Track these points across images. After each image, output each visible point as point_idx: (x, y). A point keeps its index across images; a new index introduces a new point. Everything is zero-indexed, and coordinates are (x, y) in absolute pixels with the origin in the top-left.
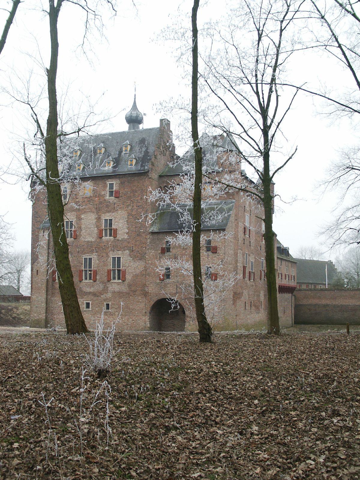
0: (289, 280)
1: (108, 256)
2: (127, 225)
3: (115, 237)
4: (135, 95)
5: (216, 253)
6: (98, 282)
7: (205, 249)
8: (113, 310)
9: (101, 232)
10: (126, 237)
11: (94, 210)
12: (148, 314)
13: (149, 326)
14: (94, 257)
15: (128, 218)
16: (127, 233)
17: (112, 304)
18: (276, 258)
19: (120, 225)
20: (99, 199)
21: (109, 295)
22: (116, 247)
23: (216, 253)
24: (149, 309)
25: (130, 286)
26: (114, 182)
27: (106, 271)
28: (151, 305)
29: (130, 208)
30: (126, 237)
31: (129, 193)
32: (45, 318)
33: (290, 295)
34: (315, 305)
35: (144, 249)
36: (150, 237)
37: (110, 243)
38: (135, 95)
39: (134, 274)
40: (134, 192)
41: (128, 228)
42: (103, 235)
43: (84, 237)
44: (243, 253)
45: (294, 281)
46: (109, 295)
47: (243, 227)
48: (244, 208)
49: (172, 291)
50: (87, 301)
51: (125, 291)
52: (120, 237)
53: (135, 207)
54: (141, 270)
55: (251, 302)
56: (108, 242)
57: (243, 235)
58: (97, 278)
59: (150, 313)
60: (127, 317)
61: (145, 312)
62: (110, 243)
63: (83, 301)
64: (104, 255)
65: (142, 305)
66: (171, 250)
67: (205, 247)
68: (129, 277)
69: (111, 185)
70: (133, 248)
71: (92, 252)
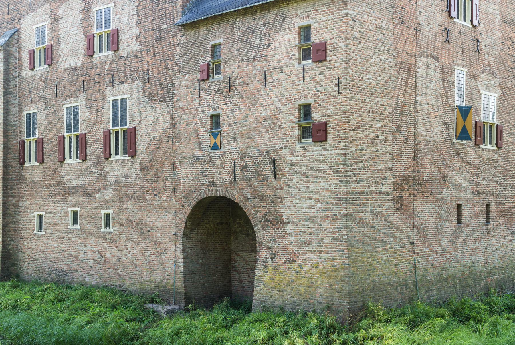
2: (137, 18)
3: (117, 50)
5: (325, 60)
6: (89, 163)
7: (297, 55)
8: (116, 228)
9: (90, 40)
10: (136, 47)
12: (180, 239)
13: (182, 269)
21: (109, 193)
23: (325, 60)
24: (182, 226)
25: (144, 168)
27: (102, 134)
28: (186, 216)
30: (136, 47)
35: (170, 72)
36: (180, 40)
37: (107, 67)
39: (152, 136)
43: (64, 59)
44: (442, 68)
46: (109, 193)
49: (225, 177)
51: (136, 182)
52: (123, 51)
54: (165, 125)
55: (488, 206)
58: (88, 152)
59: (184, 235)
61: (175, 234)
65: (169, 217)
67: (297, 48)
68: (142, 147)
70: (148, 74)
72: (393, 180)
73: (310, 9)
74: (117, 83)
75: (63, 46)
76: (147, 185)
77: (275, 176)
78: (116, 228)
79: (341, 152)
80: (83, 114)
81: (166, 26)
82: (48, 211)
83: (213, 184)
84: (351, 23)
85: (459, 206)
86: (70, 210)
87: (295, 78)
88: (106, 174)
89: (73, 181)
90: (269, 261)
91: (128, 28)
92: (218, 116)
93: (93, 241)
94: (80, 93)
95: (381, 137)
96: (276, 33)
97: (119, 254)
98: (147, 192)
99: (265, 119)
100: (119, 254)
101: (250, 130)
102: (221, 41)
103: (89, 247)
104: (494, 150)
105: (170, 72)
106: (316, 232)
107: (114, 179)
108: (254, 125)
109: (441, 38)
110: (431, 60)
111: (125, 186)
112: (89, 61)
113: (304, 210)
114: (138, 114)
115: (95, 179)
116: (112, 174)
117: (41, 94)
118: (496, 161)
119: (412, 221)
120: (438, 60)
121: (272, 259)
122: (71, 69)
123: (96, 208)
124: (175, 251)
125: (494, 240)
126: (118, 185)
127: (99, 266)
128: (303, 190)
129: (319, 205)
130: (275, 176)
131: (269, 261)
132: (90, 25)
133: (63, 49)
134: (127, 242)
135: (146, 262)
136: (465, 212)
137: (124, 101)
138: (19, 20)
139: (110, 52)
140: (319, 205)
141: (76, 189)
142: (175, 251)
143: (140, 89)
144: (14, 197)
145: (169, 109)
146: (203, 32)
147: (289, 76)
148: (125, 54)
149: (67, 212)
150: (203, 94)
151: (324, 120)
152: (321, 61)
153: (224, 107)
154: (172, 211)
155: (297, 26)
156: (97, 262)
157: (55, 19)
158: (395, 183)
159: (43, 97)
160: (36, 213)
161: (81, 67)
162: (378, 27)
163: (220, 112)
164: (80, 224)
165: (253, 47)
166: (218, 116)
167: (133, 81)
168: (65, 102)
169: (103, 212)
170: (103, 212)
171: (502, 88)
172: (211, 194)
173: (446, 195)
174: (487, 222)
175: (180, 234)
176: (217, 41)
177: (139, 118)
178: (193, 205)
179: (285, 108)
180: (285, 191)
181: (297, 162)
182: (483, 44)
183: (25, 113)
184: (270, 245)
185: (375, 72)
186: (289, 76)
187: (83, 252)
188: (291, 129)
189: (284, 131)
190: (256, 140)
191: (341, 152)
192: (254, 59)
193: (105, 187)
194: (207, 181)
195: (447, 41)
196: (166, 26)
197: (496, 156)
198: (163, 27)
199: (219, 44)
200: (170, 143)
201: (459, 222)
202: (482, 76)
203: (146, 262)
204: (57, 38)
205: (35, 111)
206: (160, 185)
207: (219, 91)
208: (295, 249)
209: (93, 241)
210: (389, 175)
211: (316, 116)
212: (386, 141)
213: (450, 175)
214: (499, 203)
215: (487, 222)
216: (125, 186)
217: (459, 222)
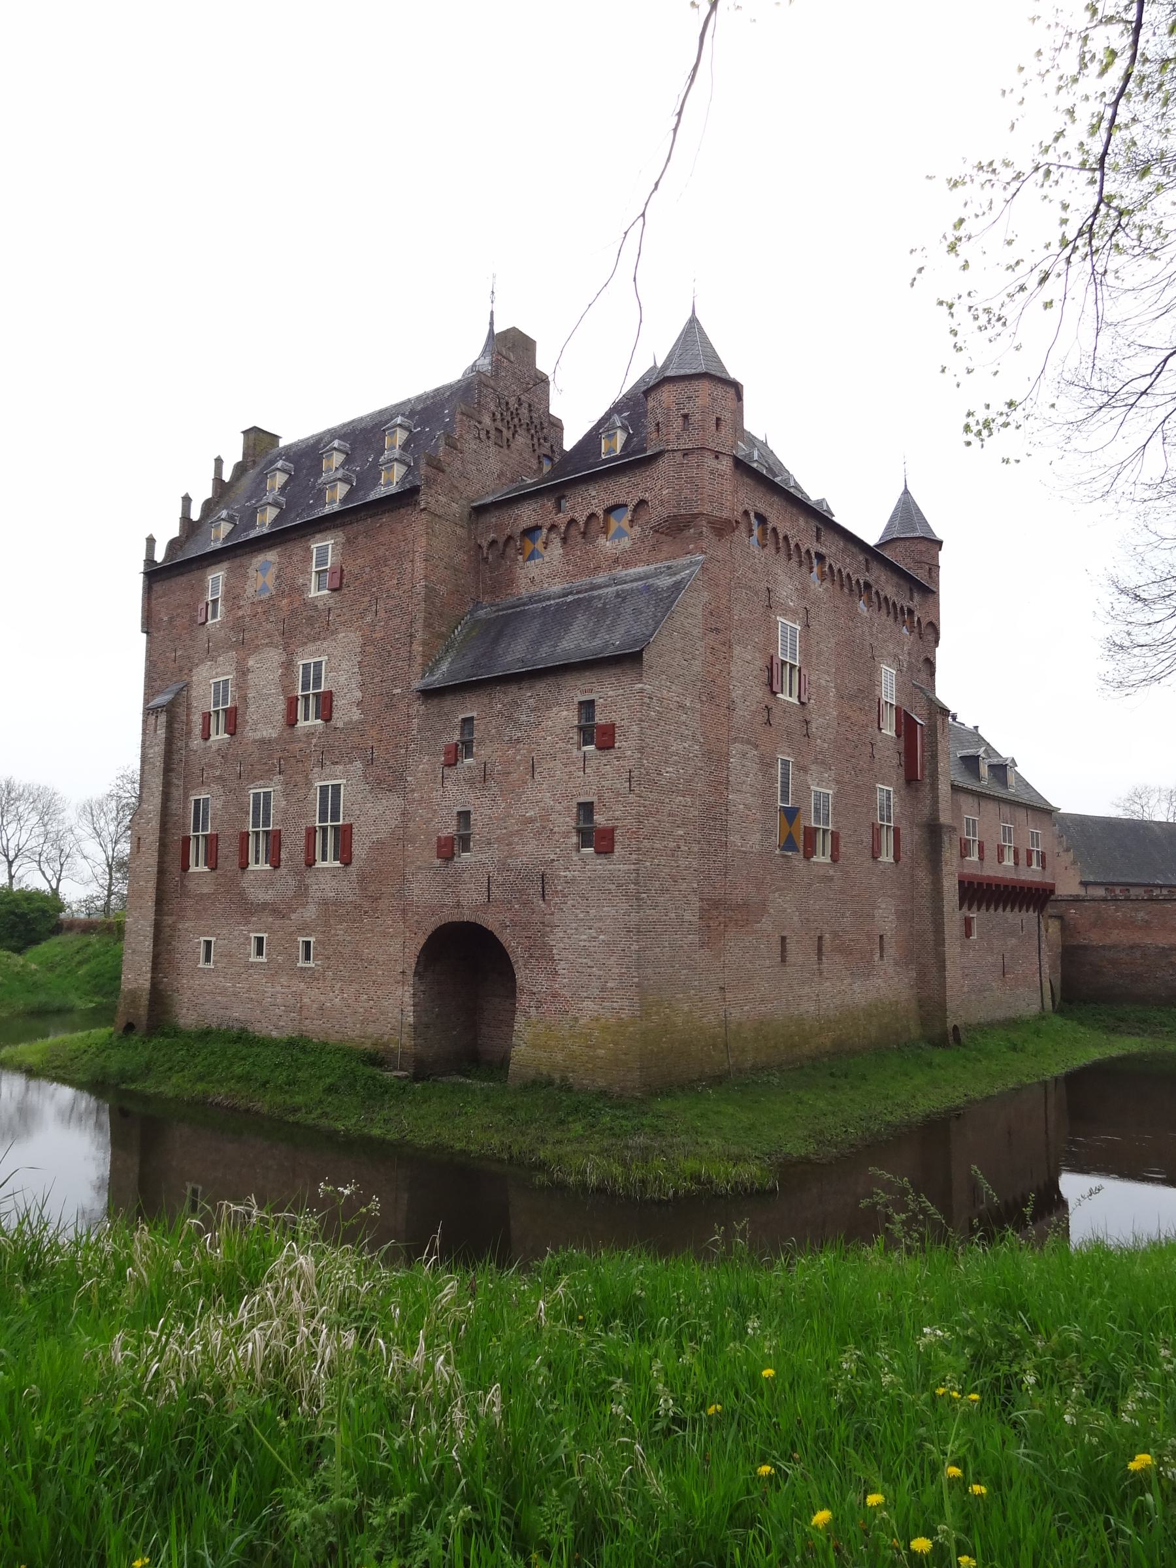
0: (1016, 864)
1: (309, 783)
2: (360, 677)
3: (328, 719)
4: (492, 313)
5: (613, 747)
6: (283, 870)
7: (576, 737)
8: (319, 962)
9: (292, 703)
10: (356, 715)
11: (278, 639)
12: (411, 979)
13: (411, 1020)
14: (274, 787)
15: (363, 652)
16: (359, 704)
17: (317, 942)
18: (944, 788)
19: (342, 679)
20: (291, 603)
21: (310, 912)
22: (327, 755)
23: (613, 747)
24: (413, 961)
25: (363, 879)
26: (330, 542)
27: (304, 832)
28: (420, 948)
29: (368, 619)
30: (356, 715)
31: (367, 569)
32: (147, 985)
33: (1032, 915)
34: (1132, 947)
35: (403, 751)
36: (418, 711)
37: (314, 741)
38: (492, 313)
39: (375, 837)
40: (379, 563)
41: (362, 685)
42: (299, 718)
43: (253, 727)
44: (762, 757)
45: (1044, 868)
46: (310, 912)
47: (760, 663)
48: (764, 596)
49: (475, 896)
50: (257, 931)
51: (350, 899)
52: (339, 719)
53: (382, 614)
54: (394, 823)
55: (820, 938)
56: (310, 735)
57: (760, 693)
58: (283, 856)
59: (416, 973)
60: (355, 986)
61: (403, 972)
62: (314, 741)
63: (249, 932)
64: (299, 778)
65: (395, 947)
66: (475, 749)
67: (576, 730)
68: (359, 849)
69: (323, 551)
70: (372, 753)
71: (267, 774)
72: (698, 904)
73: (594, 680)
74: (328, 763)
75: (252, 709)
76: (366, 905)
77: (543, 896)
78: (319, 962)
79: (633, 867)
80: (277, 803)
81: (399, 691)
82: (220, 937)
83: (458, 905)
84: (647, 700)
85: (783, 939)
86: (253, 935)
87: (573, 768)
88: (307, 887)
89: (260, 895)
90: (533, 1011)
91: (346, 690)
92: (468, 813)
93: (284, 980)
94: (274, 775)
95: (683, 848)
96: (549, 708)
97: (322, 998)
98: (366, 912)
99: (532, 820)
100: (322, 998)
101: (512, 834)
102: (474, 714)
103: (279, 988)
104: (827, 864)
105: (403, 751)
106: (598, 973)
107: (319, 894)
108: (516, 828)
109: (761, 719)
110: (747, 748)
111: (334, 904)
112: (289, 732)
113: (582, 943)
114: (356, 807)
115: (290, 893)
116: (317, 887)
117: (218, 773)
118: (831, 879)
119: (722, 959)
120: (756, 747)
121: (537, 1008)
122: (263, 741)
123: (291, 933)
124: (403, 995)
125: (828, 984)
126: (324, 903)
127: (292, 1014)
128: (581, 916)
129: (602, 937)
130: (543, 896)
131: (533, 1011)
132: (293, 683)
133: (252, 714)
134: (334, 982)
135: (361, 1010)
136: (791, 946)
137: (336, 788)
138: (191, 670)
139: (319, 721)
140: (602, 937)
141: (264, 906)
142: (403, 995)
143: (360, 773)
144: (172, 915)
145: (400, 801)
146: (448, 703)
147: (565, 765)
148: (340, 725)
149: (248, 938)
150: (446, 784)
151: (610, 824)
152: (608, 748)
153: (478, 802)
154: (400, 940)
155: (576, 700)
156: (288, 1009)
157: (243, 672)
158: (701, 909)
159: (220, 778)
160: (202, 939)
161: (277, 740)
162: (681, 706)
163: (471, 809)
164: (268, 955)
165: (517, 725)
166: (468, 813)
167: (351, 762)
168: (252, 786)
169: (301, 939)
170: (301, 939)
171: (838, 782)
172: (455, 919)
173: (766, 924)
174: (820, 959)
175: (410, 972)
176: (469, 715)
177: (358, 812)
178: (429, 933)
179: (558, 807)
180: (557, 916)
181: (574, 879)
182: (814, 725)
183: (193, 798)
184: (535, 990)
185: (676, 763)
186: (565, 765)
187: (269, 995)
188: (566, 835)
189: (556, 837)
190: (519, 847)
191: (633, 867)
192: (518, 741)
193: (304, 905)
194: (450, 901)
195: (768, 722)
196: (399, 691)
197: (831, 872)
198: (395, 691)
199: (472, 719)
200: (400, 847)
201: (783, 960)
202: (813, 767)
203: (361, 1010)
204: (244, 698)
205: (209, 796)
206: (384, 904)
207: (471, 782)
208: (568, 994)
209: (284, 980)
210: (694, 899)
211: (600, 819)
212: (690, 852)
213: (771, 896)
214: (835, 935)
215: (820, 959)
216: (334, 904)
217: (783, 960)
